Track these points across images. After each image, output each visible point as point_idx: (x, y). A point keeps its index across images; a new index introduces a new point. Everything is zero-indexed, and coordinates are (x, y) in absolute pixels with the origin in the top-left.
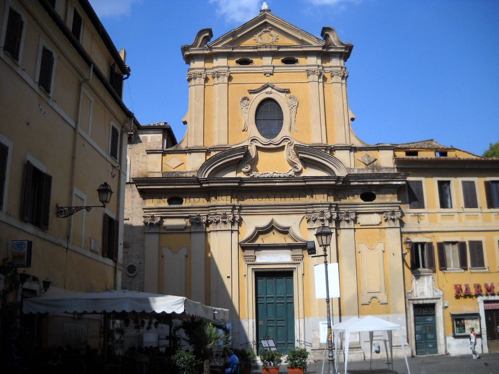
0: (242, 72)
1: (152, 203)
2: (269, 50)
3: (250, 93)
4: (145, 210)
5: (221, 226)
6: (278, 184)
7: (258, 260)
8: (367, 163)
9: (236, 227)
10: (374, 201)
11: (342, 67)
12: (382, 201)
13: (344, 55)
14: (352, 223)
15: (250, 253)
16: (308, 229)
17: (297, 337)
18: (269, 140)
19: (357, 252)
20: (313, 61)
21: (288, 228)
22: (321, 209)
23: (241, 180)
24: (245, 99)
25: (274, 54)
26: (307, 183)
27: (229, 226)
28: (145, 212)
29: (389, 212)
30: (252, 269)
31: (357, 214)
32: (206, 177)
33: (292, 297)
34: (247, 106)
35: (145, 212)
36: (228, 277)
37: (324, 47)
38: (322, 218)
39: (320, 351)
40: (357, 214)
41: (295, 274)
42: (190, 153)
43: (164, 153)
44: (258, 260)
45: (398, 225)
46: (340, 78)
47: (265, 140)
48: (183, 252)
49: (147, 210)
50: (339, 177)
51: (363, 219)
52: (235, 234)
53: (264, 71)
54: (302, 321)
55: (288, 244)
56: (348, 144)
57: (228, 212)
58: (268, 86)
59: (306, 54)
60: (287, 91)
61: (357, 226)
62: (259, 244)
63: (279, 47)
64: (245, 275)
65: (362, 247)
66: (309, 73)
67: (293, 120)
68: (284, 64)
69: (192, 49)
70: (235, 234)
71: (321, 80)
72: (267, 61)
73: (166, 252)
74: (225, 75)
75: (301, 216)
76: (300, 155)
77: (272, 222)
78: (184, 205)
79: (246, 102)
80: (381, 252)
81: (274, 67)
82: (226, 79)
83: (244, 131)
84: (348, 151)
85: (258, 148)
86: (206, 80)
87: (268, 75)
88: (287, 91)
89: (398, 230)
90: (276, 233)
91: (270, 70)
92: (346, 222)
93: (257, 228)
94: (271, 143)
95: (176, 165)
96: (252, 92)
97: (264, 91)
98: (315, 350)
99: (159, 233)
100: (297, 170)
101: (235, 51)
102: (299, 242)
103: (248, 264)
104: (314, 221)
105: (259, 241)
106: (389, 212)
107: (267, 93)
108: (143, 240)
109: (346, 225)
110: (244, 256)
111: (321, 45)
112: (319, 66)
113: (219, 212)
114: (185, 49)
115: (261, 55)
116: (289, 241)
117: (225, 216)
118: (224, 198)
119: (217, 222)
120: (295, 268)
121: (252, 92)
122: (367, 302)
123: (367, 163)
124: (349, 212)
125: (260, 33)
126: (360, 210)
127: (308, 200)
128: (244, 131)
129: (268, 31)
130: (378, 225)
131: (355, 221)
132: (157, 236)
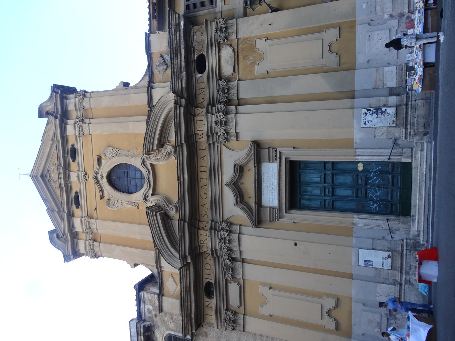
0: (86, 203)
1: (211, 317)
2: (62, 175)
3: (103, 197)
4: (219, 327)
5: (235, 246)
6: (186, 176)
8: (165, 67)
9: (236, 228)
11: (76, 97)
12: (205, 46)
13: (65, 95)
15: (266, 215)
16: (237, 140)
17: (385, 159)
18: (146, 182)
19: (268, 75)
20: (70, 129)
21: (236, 165)
22: (214, 124)
23: (182, 220)
24: (108, 204)
25: (67, 169)
26: (183, 141)
28: (221, 326)
29: (218, 35)
30: (286, 213)
33: (325, 163)
34: (116, 202)
35: (221, 326)
36: (296, 244)
37: (56, 117)
38: (224, 123)
39: (409, 126)
41: (293, 158)
42: (161, 267)
43: (161, 294)
45: (234, 21)
46: (85, 98)
47: (145, 186)
48: (265, 291)
49: (219, 324)
50: (176, 103)
51: (227, 70)
53: (83, 181)
54: (359, 152)
55: (255, 167)
56: (146, 89)
57: (218, 235)
58: (96, 178)
59: (64, 136)
60: (99, 159)
61: (236, 76)
62: (255, 203)
63: (59, 165)
64: (294, 222)
65: (261, 68)
66: (81, 134)
67: (125, 152)
68: (77, 159)
69: (67, 253)
71: (87, 121)
72: (73, 176)
73: (266, 311)
74: (89, 222)
75: (224, 148)
76: (155, 148)
77: (228, 185)
78: (213, 281)
79: (112, 202)
81: (79, 171)
82: (93, 221)
83: (138, 207)
85: (153, 194)
86: (95, 240)
87: (87, 176)
88: (99, 159)
89: (240, 21)
90: (244, 180)
91: (82, 175)
92: (230, 92)
93: (236, 204)
94: (148, 180)
95: (174, 283)
96: (102, 195)
97: (101, 182)
98: (406, 134)
99: (244, 315)
100: (173, 152)
101: (66, 211)
102: (253, 152)
103: (281, 217)
104: (228, 133)
105: (252, 202)
106: (218, 35)
107: (102, 180)
108: (253, 334)
109: (234, 91)
110: (270, 221)
111: (53, 121)
112: (75, 123)
113: (218, 245)
114: (67, 259)
115: (68, 184)
116: (251, 165)
117: (223, 240)
118: (201, 238)
119: (230, 250)
120: (286, 158)
121: (102, 195)
122: (336, 59)
123: (165, 67)
124: (218, 88)
125: (52, 183)
126: (215, 74)
127: (203, 141)
128: (138, 207)
129: (50, 174)
130: (234, 49)
131: (228, 80)
132: (248, 318)
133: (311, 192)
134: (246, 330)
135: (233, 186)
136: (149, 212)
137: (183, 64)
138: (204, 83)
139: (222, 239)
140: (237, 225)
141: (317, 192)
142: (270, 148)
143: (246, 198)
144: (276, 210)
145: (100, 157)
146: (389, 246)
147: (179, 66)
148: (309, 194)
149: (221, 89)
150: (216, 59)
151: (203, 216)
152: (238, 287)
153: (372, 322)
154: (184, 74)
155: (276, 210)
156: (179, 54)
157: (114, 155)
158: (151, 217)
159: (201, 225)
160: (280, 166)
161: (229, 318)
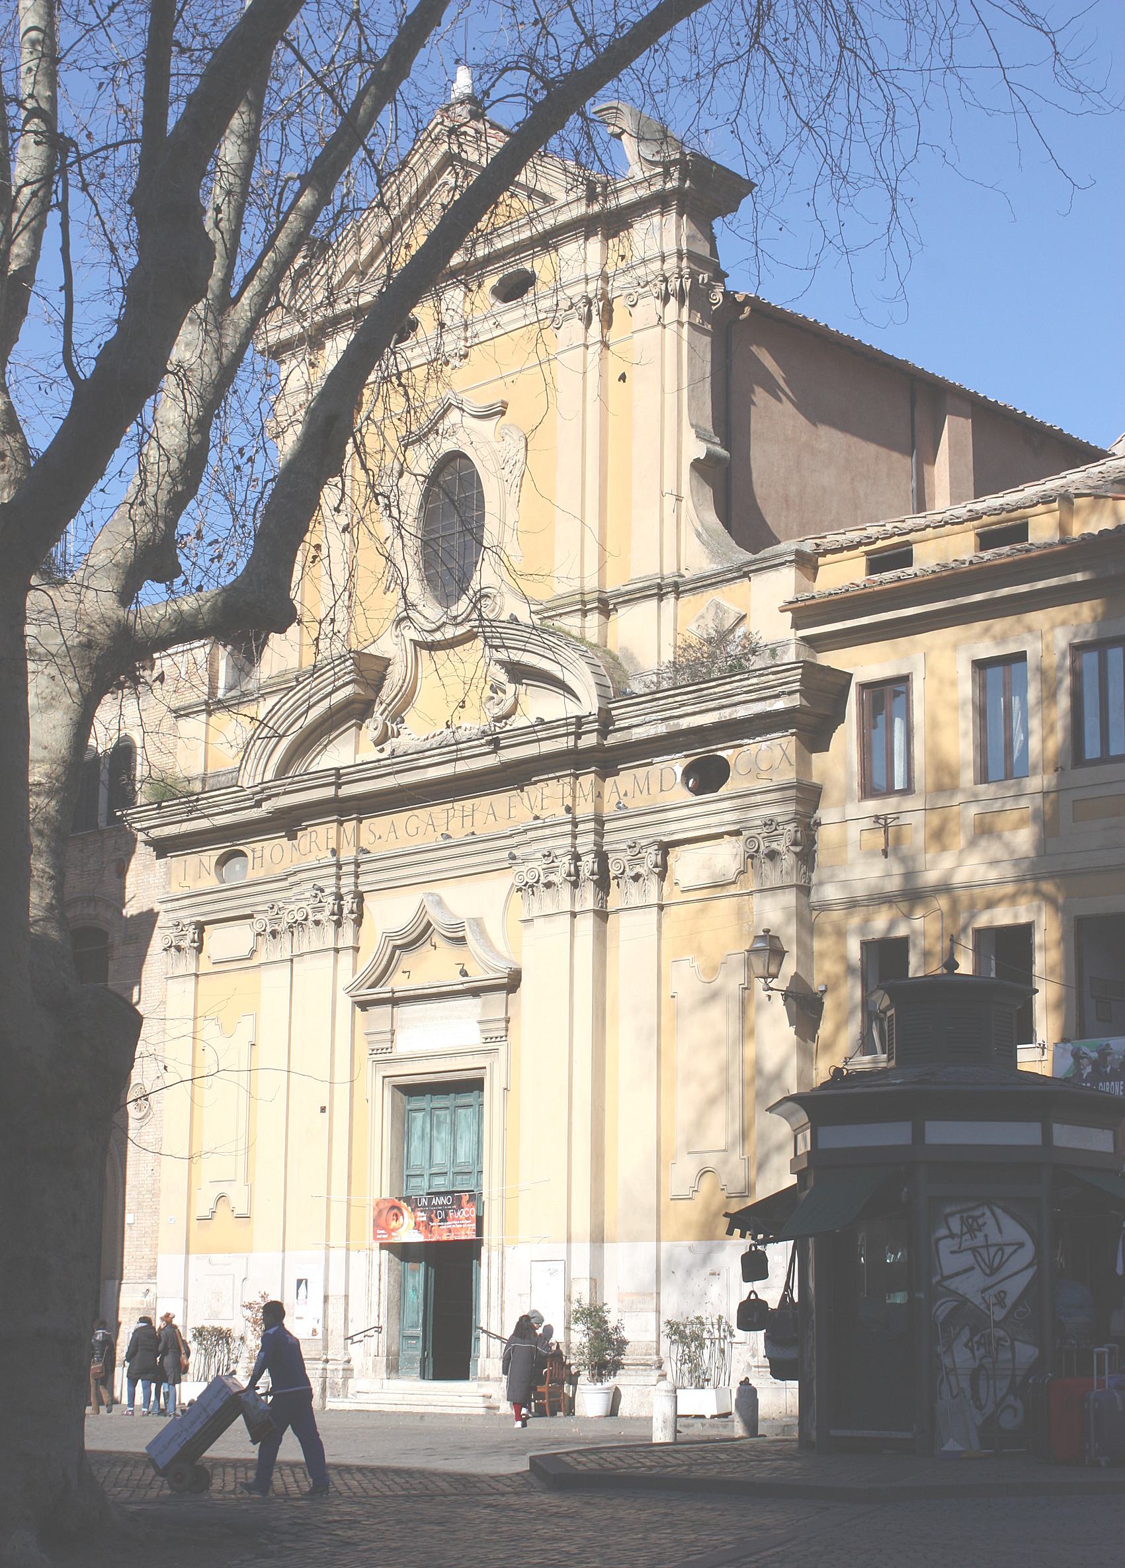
7: (402, 1047)
9: (347, 936)
10: (723, 791)
14: (653, 884)
23: (338, 776)
27: (328, 936)
30: (384, 1077)
31: (665, 848)
32: (269, 775)
40: (665, 848)
44: (402, 1047)
48: (245, 1032)
52: (346, 959)
70: (346, 959)
80: (247, 1046)
84: (653, 603)
93: (388, 937)
105: (398, 983)
110: (367, 1034)
131: (662, 871)
133: (438, 1139)
134: (170, 981)
135: (425, 921)
136: (348, 663)
137: (685, 723)
138: (662, 790)
139: (320, 902)
140: (356, 937)
141: (439, 1157)
142: (508, 1021)
143: (407, 960)
144: (389, 1050)
145: (503, 413)
146: (334, 1333)
147: (676, 712)
148: (435, 1133)
149: (639, 853)
150: (709, 826)
151: (372, 827)
152: (245, 952)
153: (218, 1300)
154: (662, 729)
155: (389, 1050)
156: (703, 706)
157: (507, 470)
158: (332, 672)
159: (350, 826)
160: (473, 1053)
161: (182, 933)
